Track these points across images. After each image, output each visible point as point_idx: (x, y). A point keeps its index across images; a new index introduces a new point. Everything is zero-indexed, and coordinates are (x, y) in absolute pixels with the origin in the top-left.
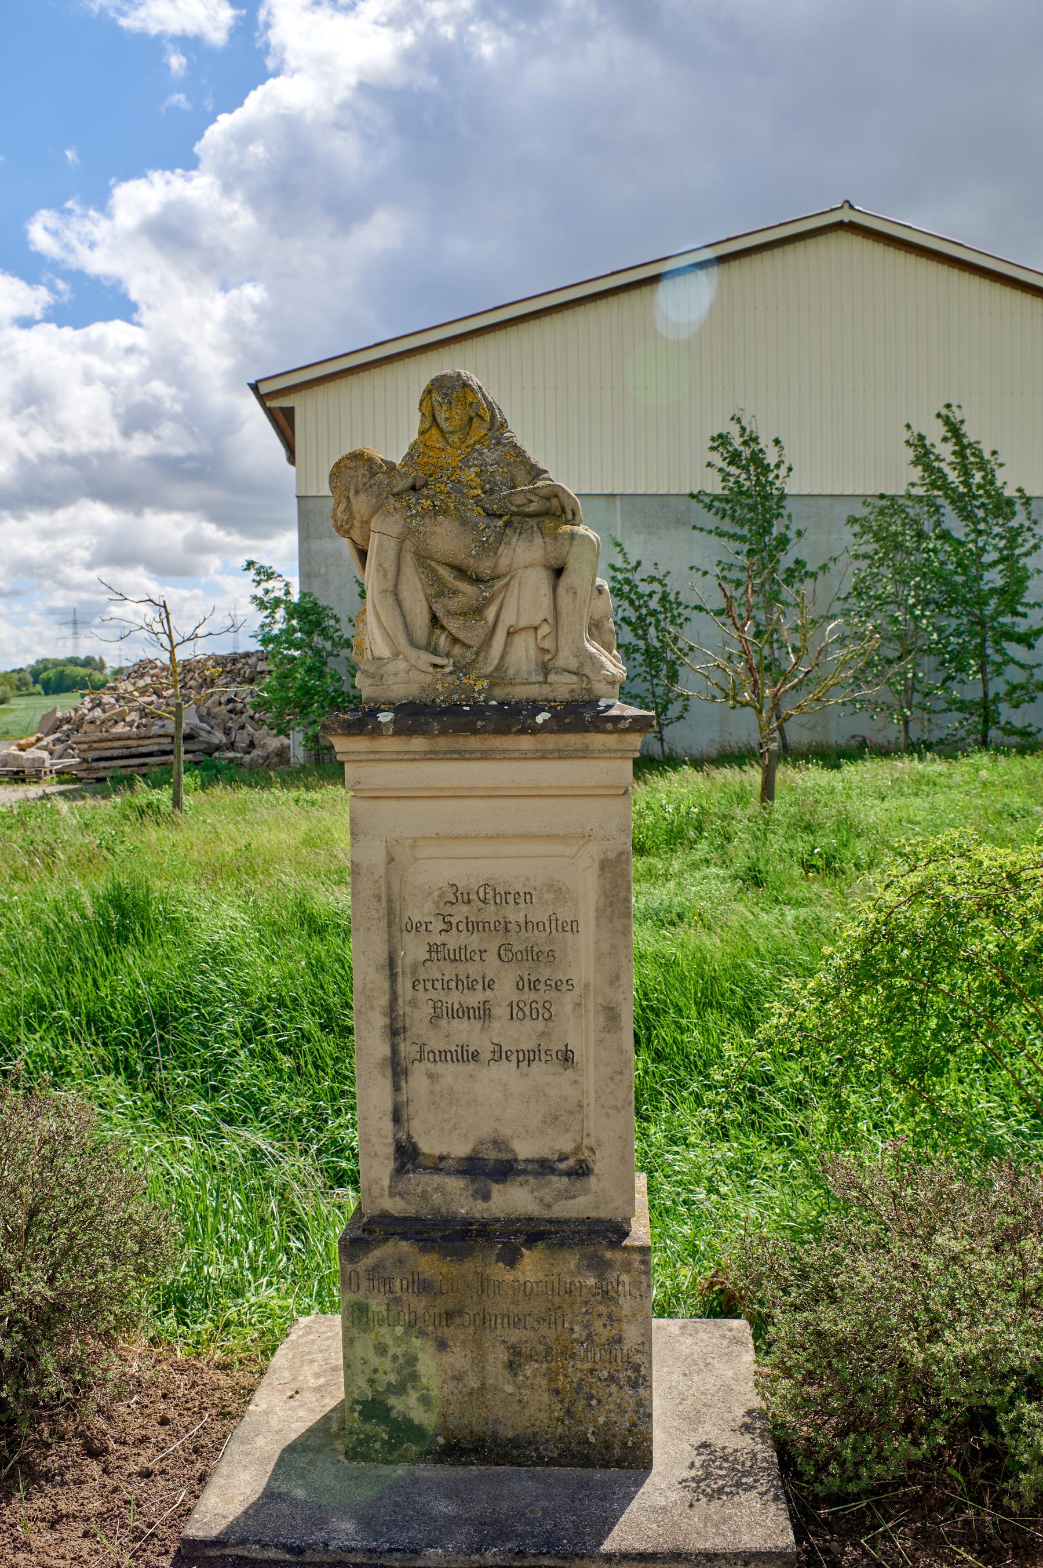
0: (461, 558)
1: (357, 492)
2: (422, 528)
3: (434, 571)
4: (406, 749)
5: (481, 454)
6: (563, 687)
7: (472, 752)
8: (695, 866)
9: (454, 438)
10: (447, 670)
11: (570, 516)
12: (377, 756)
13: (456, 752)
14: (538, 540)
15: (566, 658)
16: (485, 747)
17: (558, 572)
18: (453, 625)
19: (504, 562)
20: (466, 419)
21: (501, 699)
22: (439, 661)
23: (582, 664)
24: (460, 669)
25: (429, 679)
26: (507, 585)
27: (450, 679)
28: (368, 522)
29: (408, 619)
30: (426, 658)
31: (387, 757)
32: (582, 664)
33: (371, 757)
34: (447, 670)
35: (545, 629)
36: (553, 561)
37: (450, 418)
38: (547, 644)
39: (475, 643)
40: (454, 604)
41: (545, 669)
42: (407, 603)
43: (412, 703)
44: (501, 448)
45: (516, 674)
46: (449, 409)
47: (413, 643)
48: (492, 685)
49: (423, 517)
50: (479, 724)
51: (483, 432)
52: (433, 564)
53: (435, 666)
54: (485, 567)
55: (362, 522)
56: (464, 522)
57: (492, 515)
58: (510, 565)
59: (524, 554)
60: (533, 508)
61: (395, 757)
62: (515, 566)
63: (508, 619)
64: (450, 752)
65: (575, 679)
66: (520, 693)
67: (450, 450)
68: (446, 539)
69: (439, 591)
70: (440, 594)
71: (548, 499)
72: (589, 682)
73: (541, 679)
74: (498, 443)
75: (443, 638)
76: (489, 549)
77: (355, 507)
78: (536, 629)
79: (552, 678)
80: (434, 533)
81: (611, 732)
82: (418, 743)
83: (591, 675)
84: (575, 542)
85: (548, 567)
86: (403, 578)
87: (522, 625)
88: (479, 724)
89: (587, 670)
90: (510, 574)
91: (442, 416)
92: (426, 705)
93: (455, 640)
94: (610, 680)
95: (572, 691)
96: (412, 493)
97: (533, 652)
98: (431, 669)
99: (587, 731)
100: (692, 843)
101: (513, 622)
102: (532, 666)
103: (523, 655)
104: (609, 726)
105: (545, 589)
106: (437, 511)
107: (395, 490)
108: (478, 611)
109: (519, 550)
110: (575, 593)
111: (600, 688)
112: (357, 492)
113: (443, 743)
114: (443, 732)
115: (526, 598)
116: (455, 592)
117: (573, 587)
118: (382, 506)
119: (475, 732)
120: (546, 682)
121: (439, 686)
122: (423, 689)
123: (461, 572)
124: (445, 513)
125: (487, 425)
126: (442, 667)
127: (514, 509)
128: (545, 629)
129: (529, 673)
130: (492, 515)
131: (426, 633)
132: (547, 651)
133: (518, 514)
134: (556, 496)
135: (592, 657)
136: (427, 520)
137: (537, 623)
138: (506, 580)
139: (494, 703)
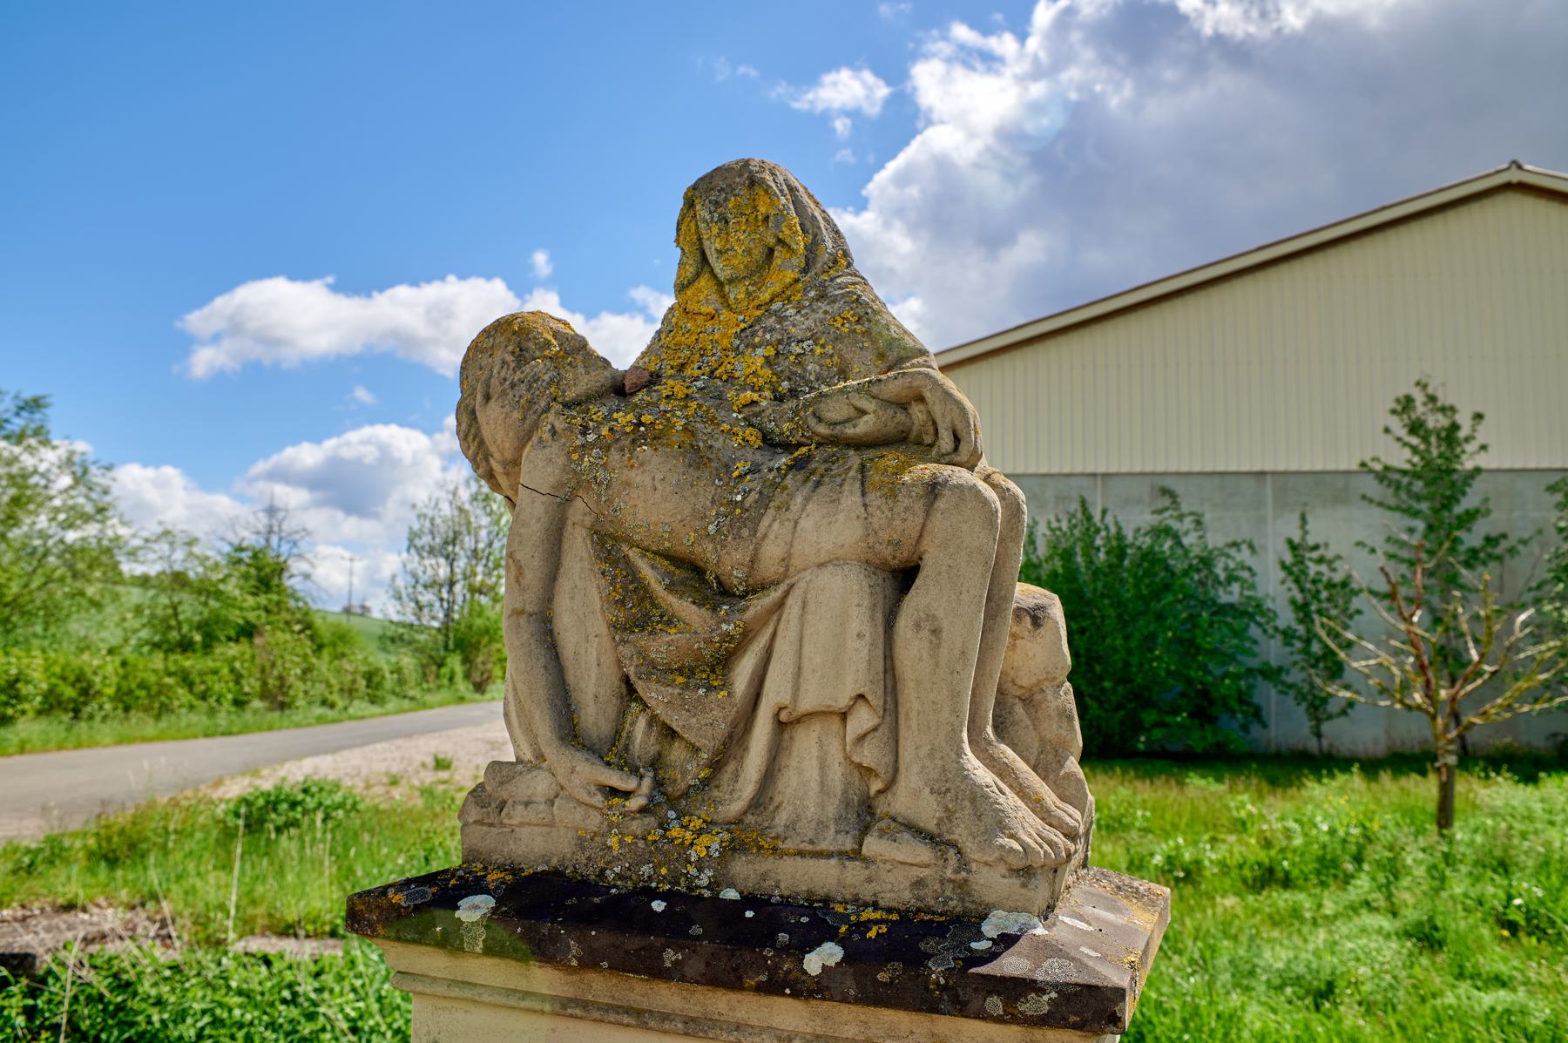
0: (686, 542)
1: (487, 398)
2: (601, 474)
3: (633, 575)
4: (523, 985)
5: (781, 319)
6: (895, 873)
7: (665, 1017)
8: (1354, 909)
9: (737, 293)
10: (635, 803)
11: (946, 443)
12: (468, 994)
13: (628, 1010)
14: (851, 498)
15: (913, 798)
16: (694, 1010)
17: (904, 576)
18: (655, 694)
19: (772, 551)
20: (758, 253)
21: (750, 886)
22: (615, 779)
23: (949, 815)
24: (672, 802)
25: (594, 821)
26: (780, 605)
27: (636, 826)
28: (516, 462)
29: (571, 678)
30: (587, 772)
31: (485, 997)
32: (949, 815)
33: (456, 992)
34: (635, 803)
35: (863, 719)
36: (887, 552)
37: (733, 251)
38: (869, 755)
39: (708, 743)
40: (661, 646)
41: (865, 814)
42: (569, 641)
43: (557, 873)
44: (823, 306)
45: (791, 826)
46: (724, 232)
47: (570, 732)
48: (735, 848)
49: (607, 449)
50: (670, 956)
51: (790, 275)
52: (633, 554)
53: (613, 792)
54: (731, 563)
55: (505, 463)
56: (697, 457)
57: (771, 443)
58: (786, 560)
59: (820, 535)
60: (864, 426)
61: (503, 1000)
62: (797, 561)
63: (775, 693)
64: (618, 1009)
65: (924, 853)
66: (796, 876)
67: (725, 315)
68: (656, 497)
69: (635, 613)
70: (641, 623)
71: (904, 406)
72: (964, 865)
73: (848, 844)
74: (822, 297)
75: (642, 723)
76: (741, 520)
77: (486, 433)
78: (844, 716)
79: (872, 845)
80: (628, 484)
81: (999, 1020)
82: (543, 979)
83: (970, 847)
84: (941, 504)
85: (874, 565)
86: (564, 585)
87: (806, 705)
88: (670, 956)
89: (960, 834)
90: (784, 578)
91: (712, 246)
92: (584, 882)
93: (670, 734)
94: (1018, 863)
95: (919, 883)
96: (614, 402)
97: (837, 772)
98: (598, 800)
99: (933, 1009)
100: (1347, 879)
101: (786, 699)
102: (832, 809)
103: (812, 778)
104: (995, 1004)
105: (860, 622)
106: (640, 435)
107: (571, 394)
108: (723, 662)
109: (806, 524)
110: (936, 632)
111: (990, 882)
112: (487, 398)
113: (600, 986)
114: (589, 962)
115: (819, 642)
116: (669, 621)
117: (931, 617)
118: (535, 426)
119: (658, 973)
120: (856, 855)
121: (613, 841)
122: (581, 843)
123: (692, 574)
124: (657, 438)
125: (798, 261)
126: (627, 795)
127: (822, 429)
128: (863, 719)
129: (822, 825)
130: (771, 443)
131: (612, 711)
132: (867, 772)
133: (834, 441)
134: (921, 399)
135: (977, 796)
136: (615, 455)
137: (843, 702)
138: (774, 595)
139: (731, 894)
